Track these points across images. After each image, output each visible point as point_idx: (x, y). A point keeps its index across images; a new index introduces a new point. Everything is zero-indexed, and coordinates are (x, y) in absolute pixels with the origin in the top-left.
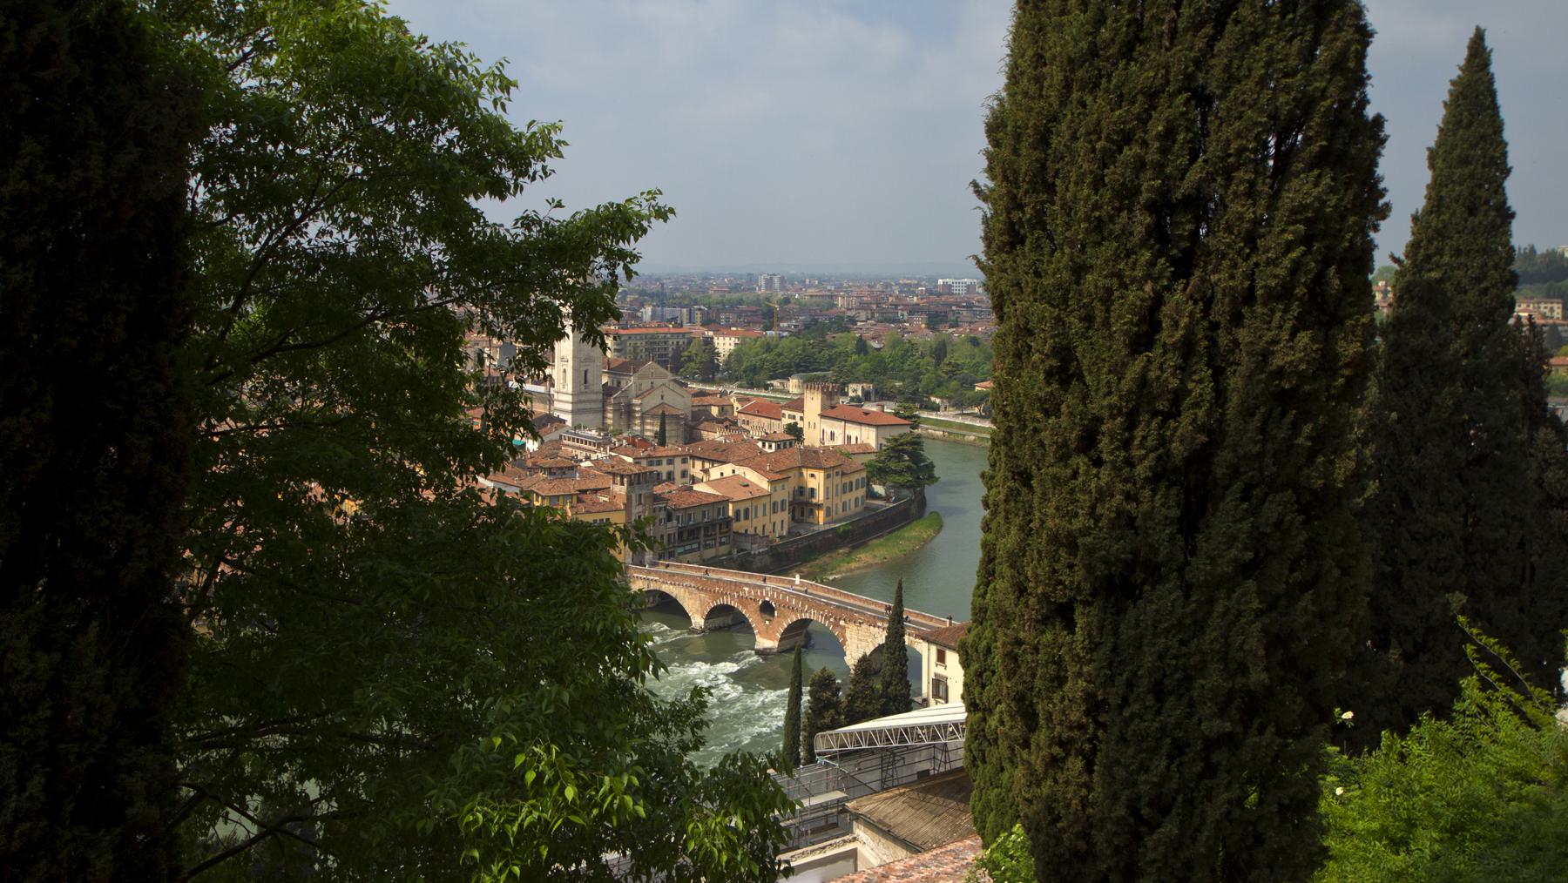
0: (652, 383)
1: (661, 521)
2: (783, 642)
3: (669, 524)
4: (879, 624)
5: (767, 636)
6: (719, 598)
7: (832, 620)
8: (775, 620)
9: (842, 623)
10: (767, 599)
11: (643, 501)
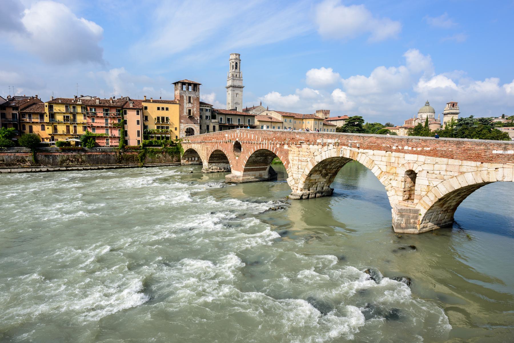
1: (207, 117)
2: (249, 173)
3: (213, 121)
7: (278, 146)
9: (286, 147)
10: (237, 140)
11: (192, 101)
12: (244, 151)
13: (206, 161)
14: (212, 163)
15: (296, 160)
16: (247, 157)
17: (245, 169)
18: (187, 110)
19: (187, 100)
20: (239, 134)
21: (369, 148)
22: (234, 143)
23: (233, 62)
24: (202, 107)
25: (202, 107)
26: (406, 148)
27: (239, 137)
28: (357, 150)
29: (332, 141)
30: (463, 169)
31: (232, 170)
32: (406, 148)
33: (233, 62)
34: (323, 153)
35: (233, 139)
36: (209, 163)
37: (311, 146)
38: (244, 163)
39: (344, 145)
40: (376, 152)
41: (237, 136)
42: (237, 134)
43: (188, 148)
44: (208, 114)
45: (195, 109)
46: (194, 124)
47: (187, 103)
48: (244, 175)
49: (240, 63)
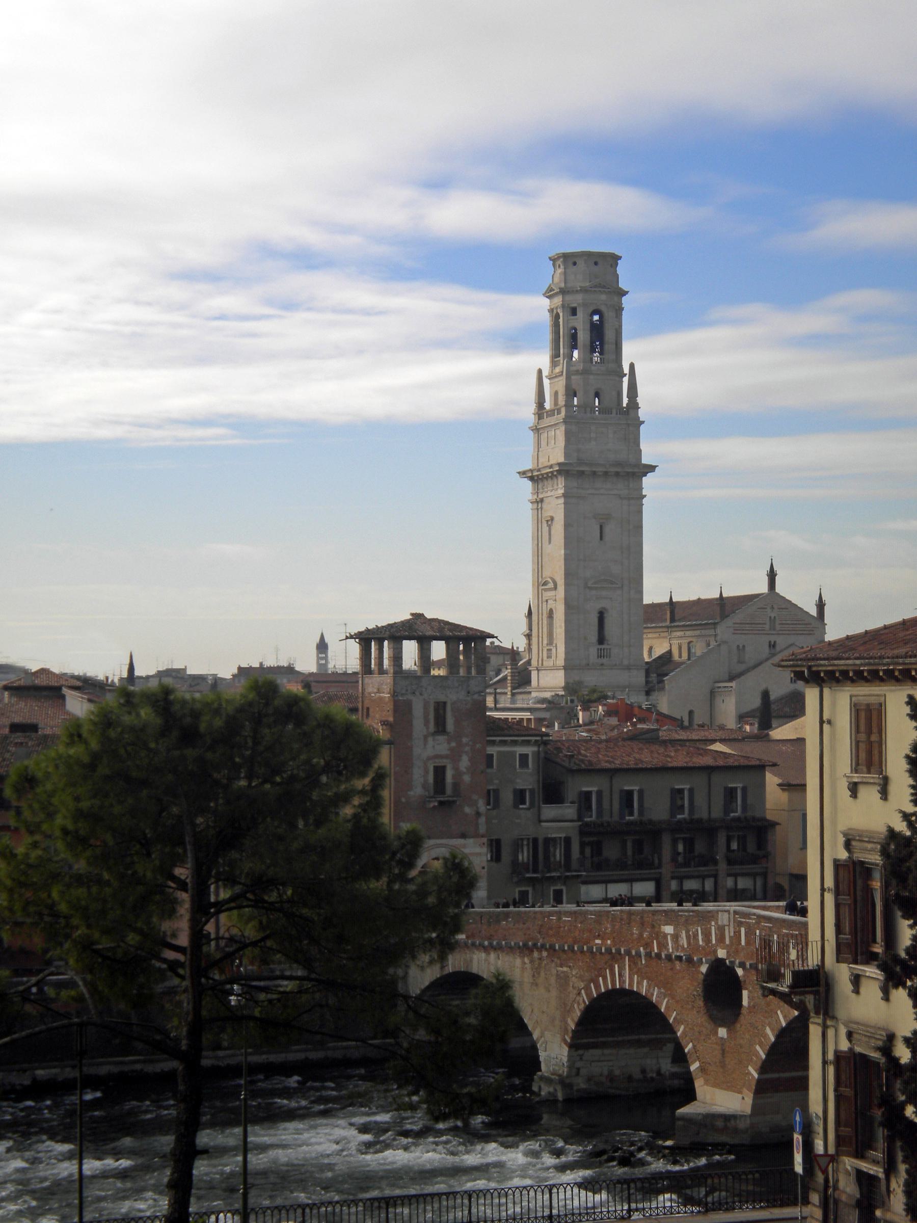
0: (772, 645)
1: (520, 796)
3: (550, 811)
8: (745, 1018)
10: (722, 953)
13: (558, 1038)
14: (587, 1047)
16: (768, 1031)
17: (759, 1081)
18: (426, 772)
19: (426, 723)
20: (729, 933)
22: (704, 969)
23: (574, 312)
24: (491, 750)
25: (491, 750)
27: (727, 942)
31: (699, 1084)
33: (574, 312)
36: (573, 1046)
38: (757, 1054)
41: (721, 939)
42: (721, 930)
43: (446, 972)
44: (527, 780)
45: (465, 762)
46: (463, 836)
47: (426, 737)
48: (756, 1108)
49: (619, 310)
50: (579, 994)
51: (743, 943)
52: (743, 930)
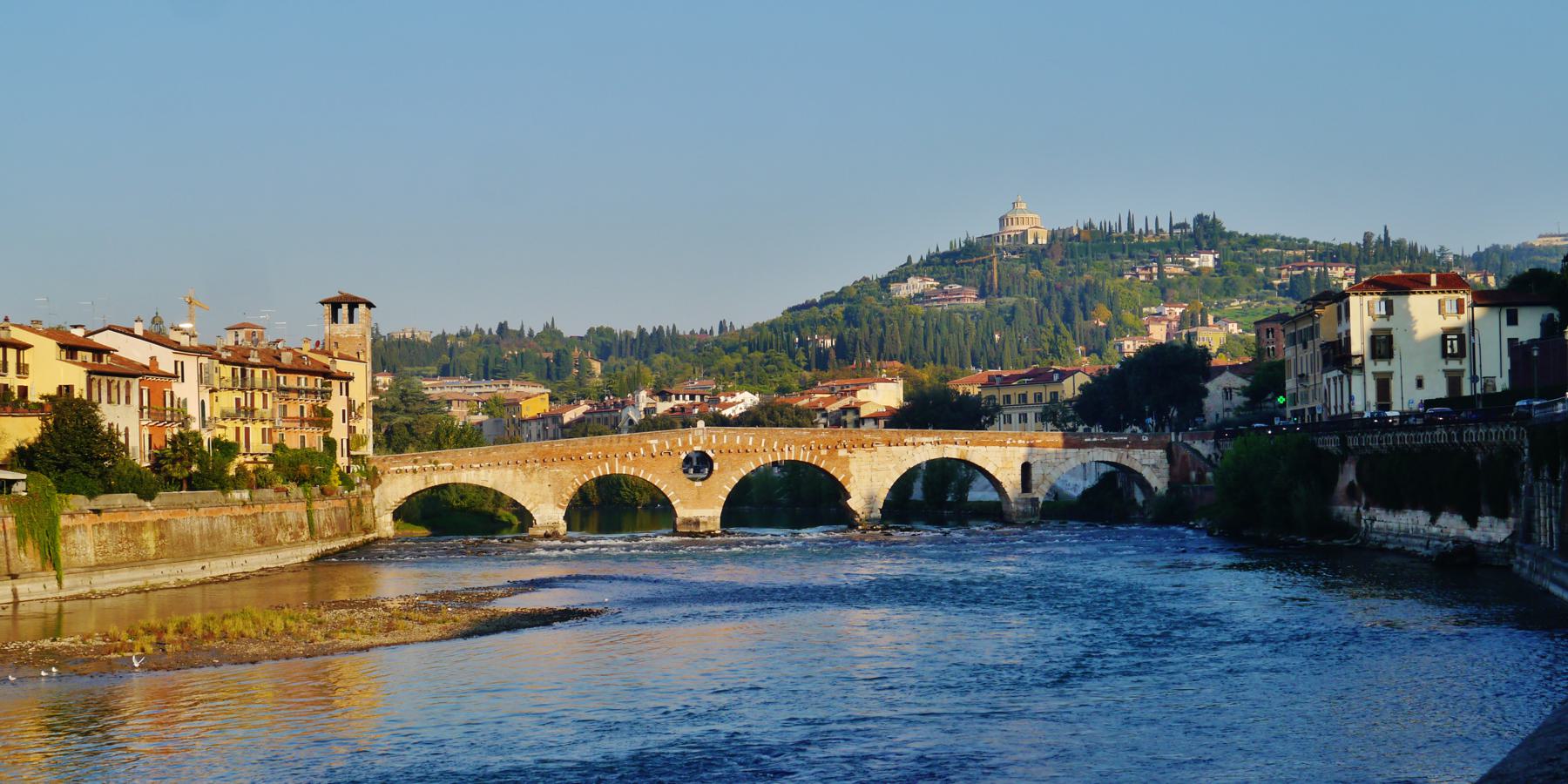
4: (909, 440)
5: (699, 501)
6: (591, 468)
7: (824, 452)
9: (842, 453)
10: (697, 448)
12: (719, 471)
13: (552, 505)
15: (866, 470)
21: (980, 444)
26: (1020, 441)
27: (702, 442)
28: (965, 447)
29: (931, 439)
30: (1068, 456)
32: (1020, 441)
34: (916, 455)
35: (679, 448)
37: (894, 448)
39: (947, 443)
40: (989, 448)
50: (573, 481)
51: (714, 441)
52: (714, 437)
